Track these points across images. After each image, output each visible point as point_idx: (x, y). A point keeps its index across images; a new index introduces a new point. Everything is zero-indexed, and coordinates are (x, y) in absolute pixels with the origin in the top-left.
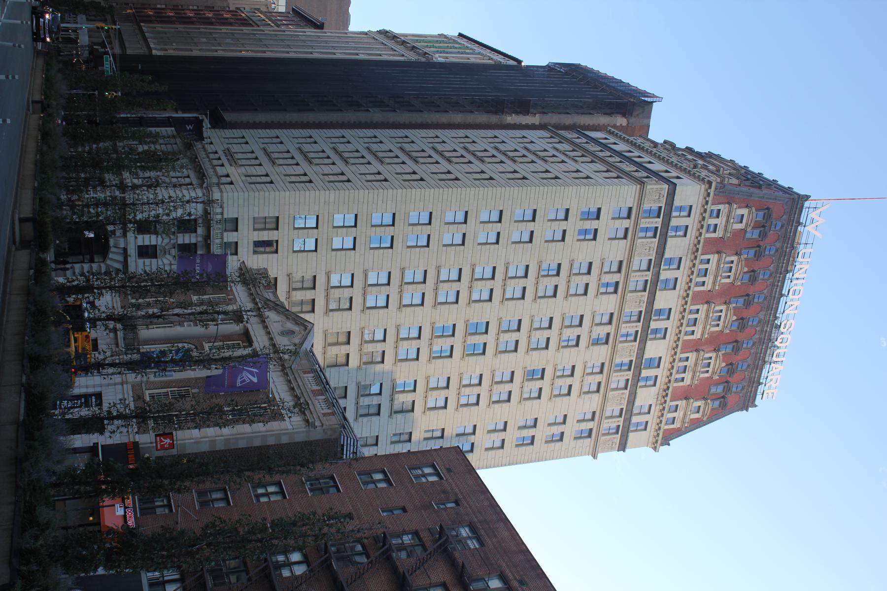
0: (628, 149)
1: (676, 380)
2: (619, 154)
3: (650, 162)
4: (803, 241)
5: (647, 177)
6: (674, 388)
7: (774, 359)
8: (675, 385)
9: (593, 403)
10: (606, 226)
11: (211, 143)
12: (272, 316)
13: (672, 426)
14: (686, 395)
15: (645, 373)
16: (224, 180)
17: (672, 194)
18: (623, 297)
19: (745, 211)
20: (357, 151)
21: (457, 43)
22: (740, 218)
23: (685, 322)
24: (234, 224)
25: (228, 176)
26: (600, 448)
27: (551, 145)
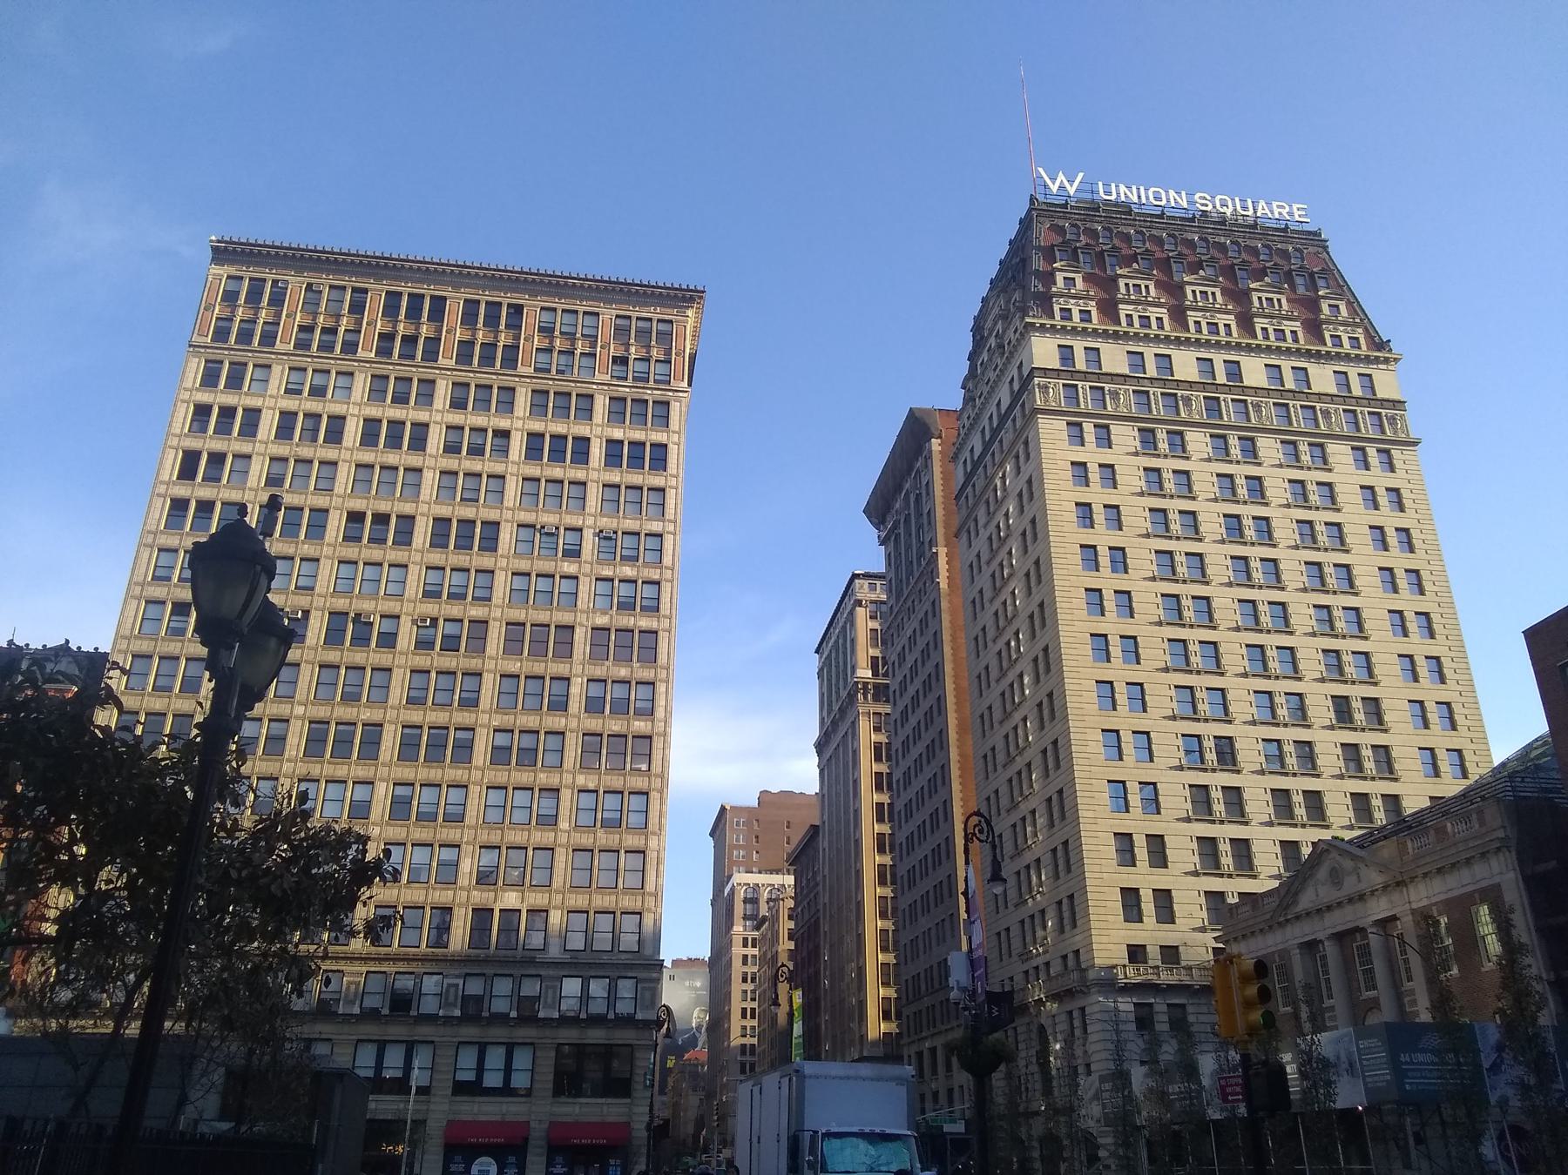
0: (979, 434)
1: (1296, 340)
2: (987, 446)
3: (999, 404)
4: (1089, 196)
5: (1023, 405)
6: (1306, 343)
7: (1250, 213)
8: (1302, 341)
9: (1340, 453)
10: (1092, 454)
11: (1011, 979)
12: (1306, 901)
13: (1362, 341)
14: (1314, 328)
15: (1290, 384)
16: (1071, 962)
17: (1045, 372)
18: (1186, 424)
19: (1059, 277)
20: (1010, 780)
21: (829, 655)
22: (1070, 281)
23: (1214, 338)
24: (1136, 953)
25: (1065, 957)
26: (1402, 436)
27: (981, 531)
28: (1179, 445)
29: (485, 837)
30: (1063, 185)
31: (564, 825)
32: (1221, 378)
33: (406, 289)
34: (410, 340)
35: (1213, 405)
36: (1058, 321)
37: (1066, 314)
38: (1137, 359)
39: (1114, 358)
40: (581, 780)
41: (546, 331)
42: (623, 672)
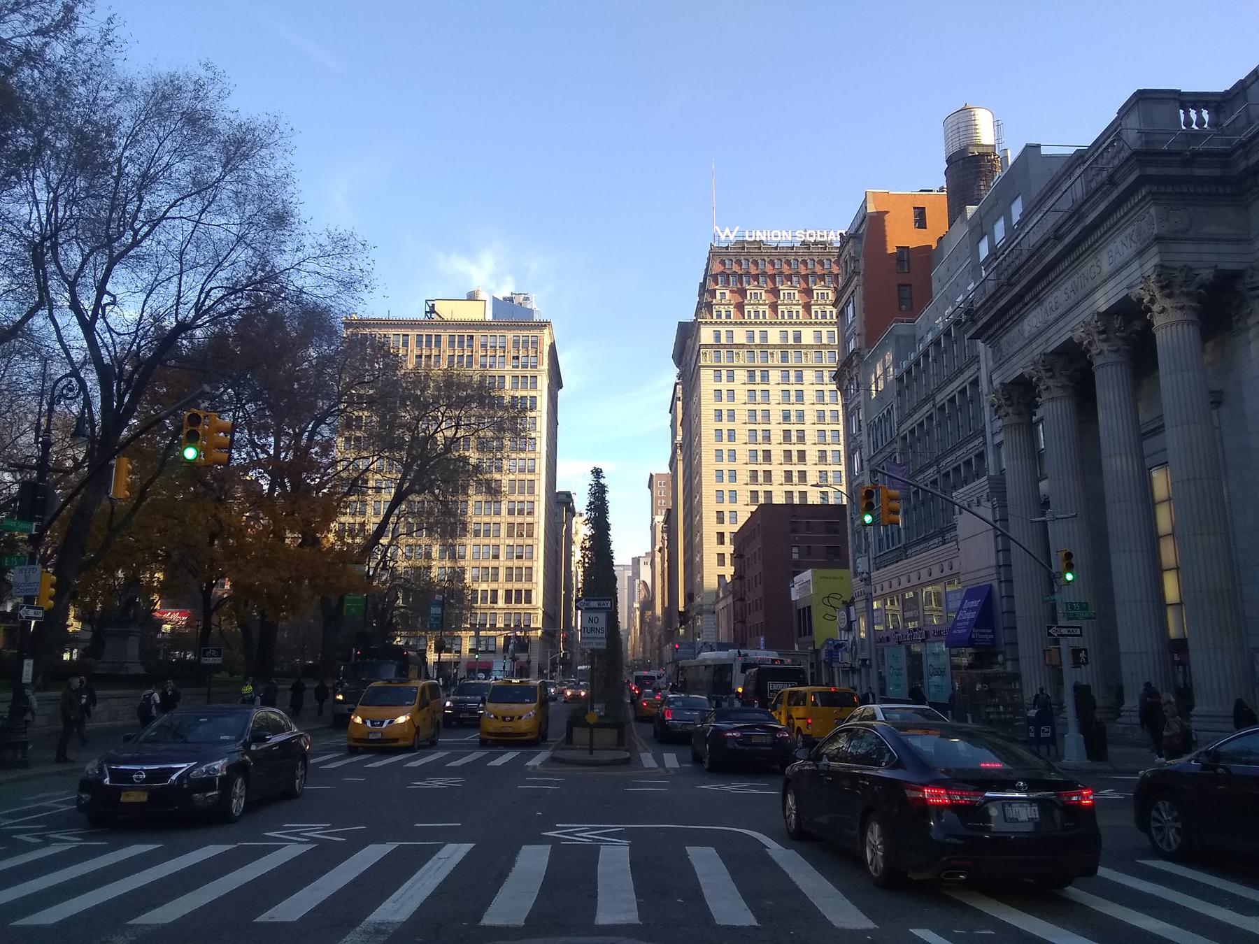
17: (706, 346)
28: (765, 378)
29: (473, 564)
30: (728, 235)
31: (501, 558)
32: (791, 341)
33: (424, 332)
34: (429, 357)
35: (785, 357)
36: (715, 319)
37: (719, 316)
38: (751, 335)
39: (740, 336)
40: (507, 542)
41: (484, 346)
42: (521, 498)
